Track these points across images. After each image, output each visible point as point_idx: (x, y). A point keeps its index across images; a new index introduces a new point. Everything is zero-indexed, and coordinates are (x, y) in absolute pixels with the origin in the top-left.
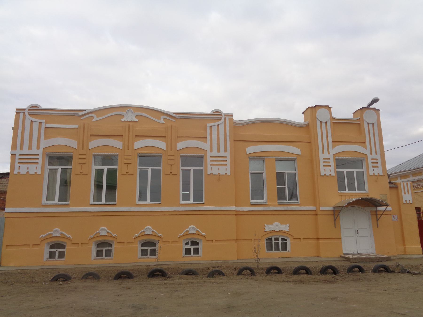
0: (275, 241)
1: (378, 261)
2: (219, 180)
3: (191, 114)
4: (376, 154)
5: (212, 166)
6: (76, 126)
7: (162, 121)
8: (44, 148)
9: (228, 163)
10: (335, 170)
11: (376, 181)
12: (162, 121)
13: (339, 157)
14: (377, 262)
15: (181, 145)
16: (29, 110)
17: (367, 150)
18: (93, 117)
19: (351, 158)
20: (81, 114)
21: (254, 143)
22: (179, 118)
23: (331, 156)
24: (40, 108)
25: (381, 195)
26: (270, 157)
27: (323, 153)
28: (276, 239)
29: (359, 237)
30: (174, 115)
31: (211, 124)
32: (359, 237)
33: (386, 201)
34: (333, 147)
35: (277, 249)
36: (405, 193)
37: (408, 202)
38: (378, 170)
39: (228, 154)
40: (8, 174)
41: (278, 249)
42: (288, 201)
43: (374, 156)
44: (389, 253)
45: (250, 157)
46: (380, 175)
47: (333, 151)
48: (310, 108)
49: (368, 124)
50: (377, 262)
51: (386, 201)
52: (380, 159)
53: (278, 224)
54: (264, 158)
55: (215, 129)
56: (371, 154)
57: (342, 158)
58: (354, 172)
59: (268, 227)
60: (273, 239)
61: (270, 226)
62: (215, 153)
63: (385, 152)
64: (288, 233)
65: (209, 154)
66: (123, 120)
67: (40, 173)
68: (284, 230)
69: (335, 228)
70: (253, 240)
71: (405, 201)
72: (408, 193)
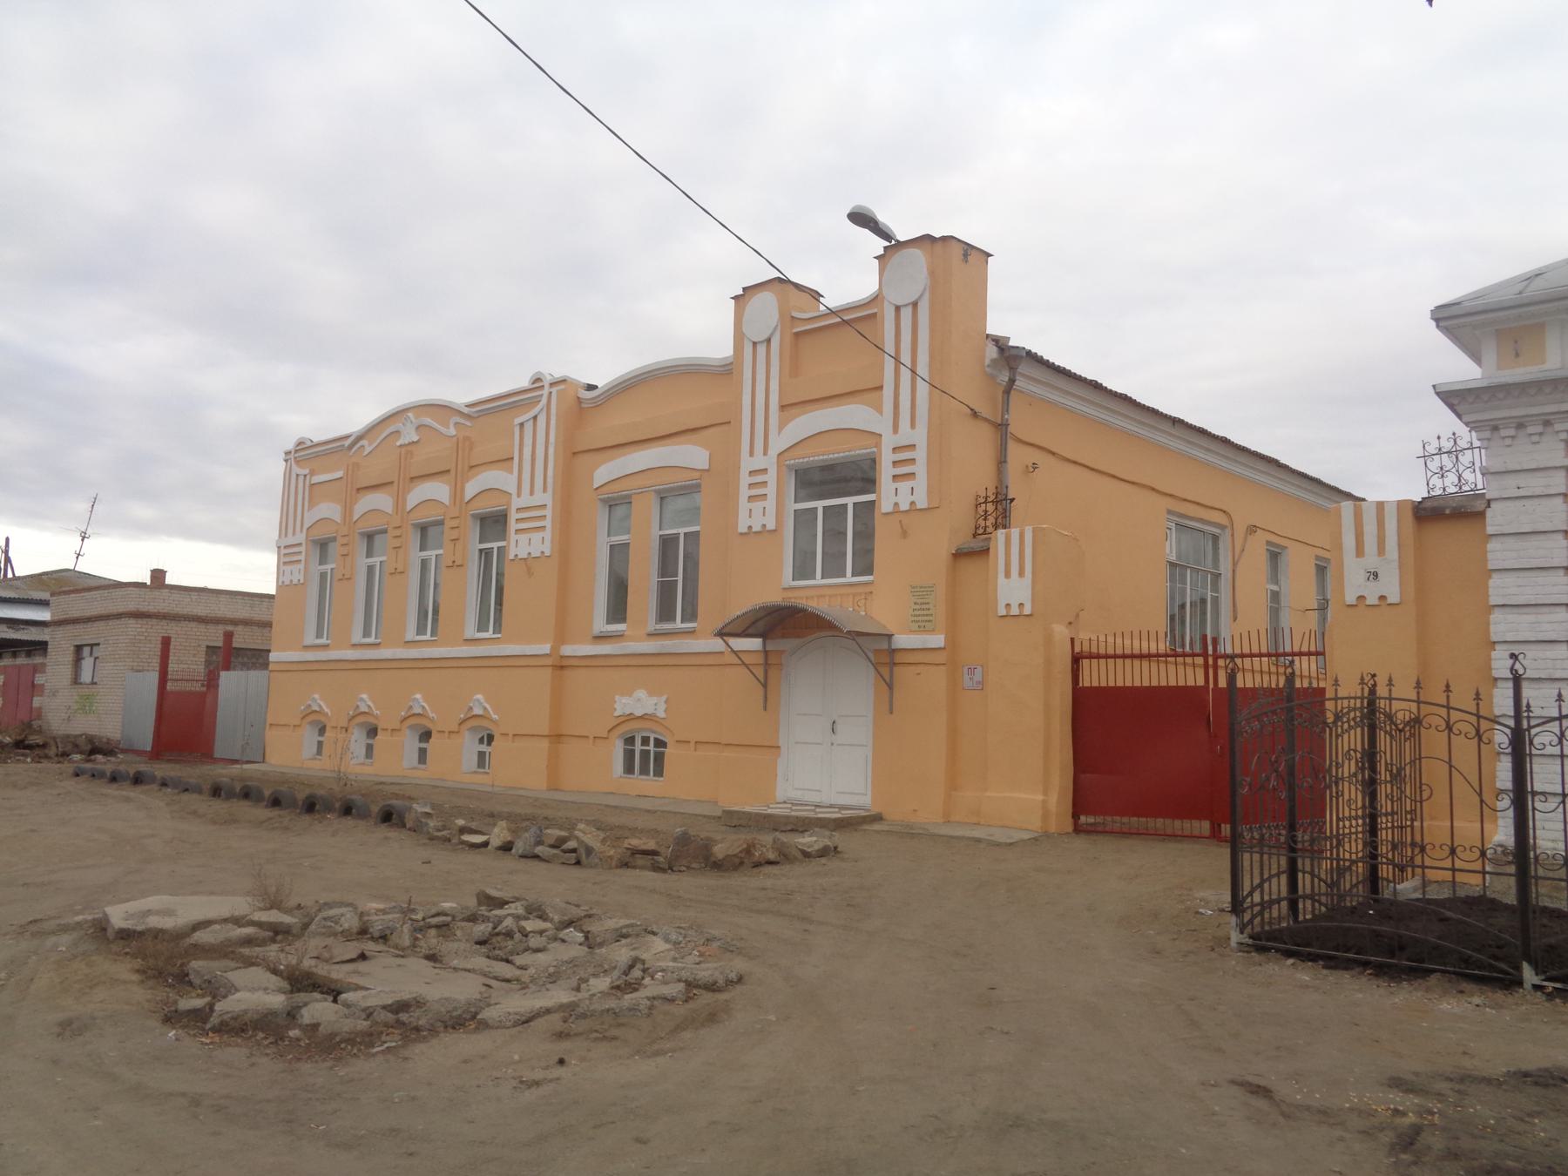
0: (642, 745)
1: (792, 830)
2: (530, 572)
3: (489, 400)
4: (913, 425)
5: (750, 505)
6: (339, 474)
7: (452, 431)
8: (780, 454)
9: (548, 523)
10: (879, 497)
11: (904, 534)
12: (452, 431)
13: (828, 454)
14: (790, 831)
15: (471, 489)
16: (296, 451)
17: (882, 415)
18: (363, 446)
19: (831, 456)
20: (347, 443)
21: (615, 451)
22: (476, 415)
23: (770, 462)
24: (309, 444)
25: (914, 588)
26: (640, 490)
27: (751, 454)
28: (645, 741)
29: (839, 745)
30: (466, 410)
31: (518, 420)
32: (839, 745)
33: (929, 609)
34: (782, 426)
35: (644, 770)
36: (1008, 575)
37: (1015, 611)
38: (751, 510)
39: (547, 498)
40: (274, 595)
41: (647, 773)
42: (679, 624)
43: (906, 435)
44: (915, 811)
45: (788, 462)
46: (902, 512)
47: (779, 443)
48: (778, 286)
49: (755, 344)
50: (790, 831)
51: (929, 609)
52: (925, 449)
53: (641, 694)
54: (629, 496)
55: (529, 427)
56: (519, 495)
57: (806, 460)
58: (796, 508)
59: (625, 704)
60: (638, 741)
61: (625, 700)
62: (526, 500)
63: (17, 575)
64: (661, 721)
65: (516, 503)
66: (366, 453)
67: (773, 528)
68: (653, 715)
69: (765, 709)
70: (511, 736)
71: (1004, 605)
72: (1021, 574)
